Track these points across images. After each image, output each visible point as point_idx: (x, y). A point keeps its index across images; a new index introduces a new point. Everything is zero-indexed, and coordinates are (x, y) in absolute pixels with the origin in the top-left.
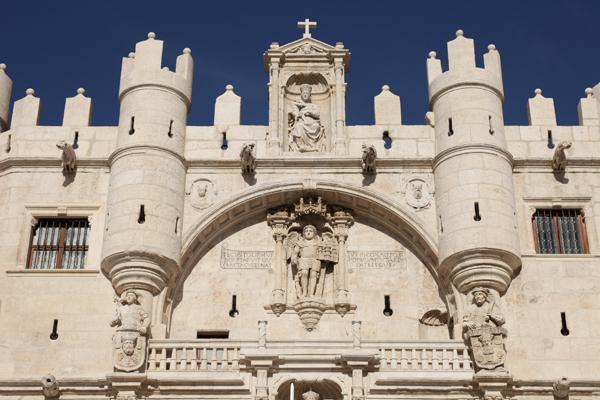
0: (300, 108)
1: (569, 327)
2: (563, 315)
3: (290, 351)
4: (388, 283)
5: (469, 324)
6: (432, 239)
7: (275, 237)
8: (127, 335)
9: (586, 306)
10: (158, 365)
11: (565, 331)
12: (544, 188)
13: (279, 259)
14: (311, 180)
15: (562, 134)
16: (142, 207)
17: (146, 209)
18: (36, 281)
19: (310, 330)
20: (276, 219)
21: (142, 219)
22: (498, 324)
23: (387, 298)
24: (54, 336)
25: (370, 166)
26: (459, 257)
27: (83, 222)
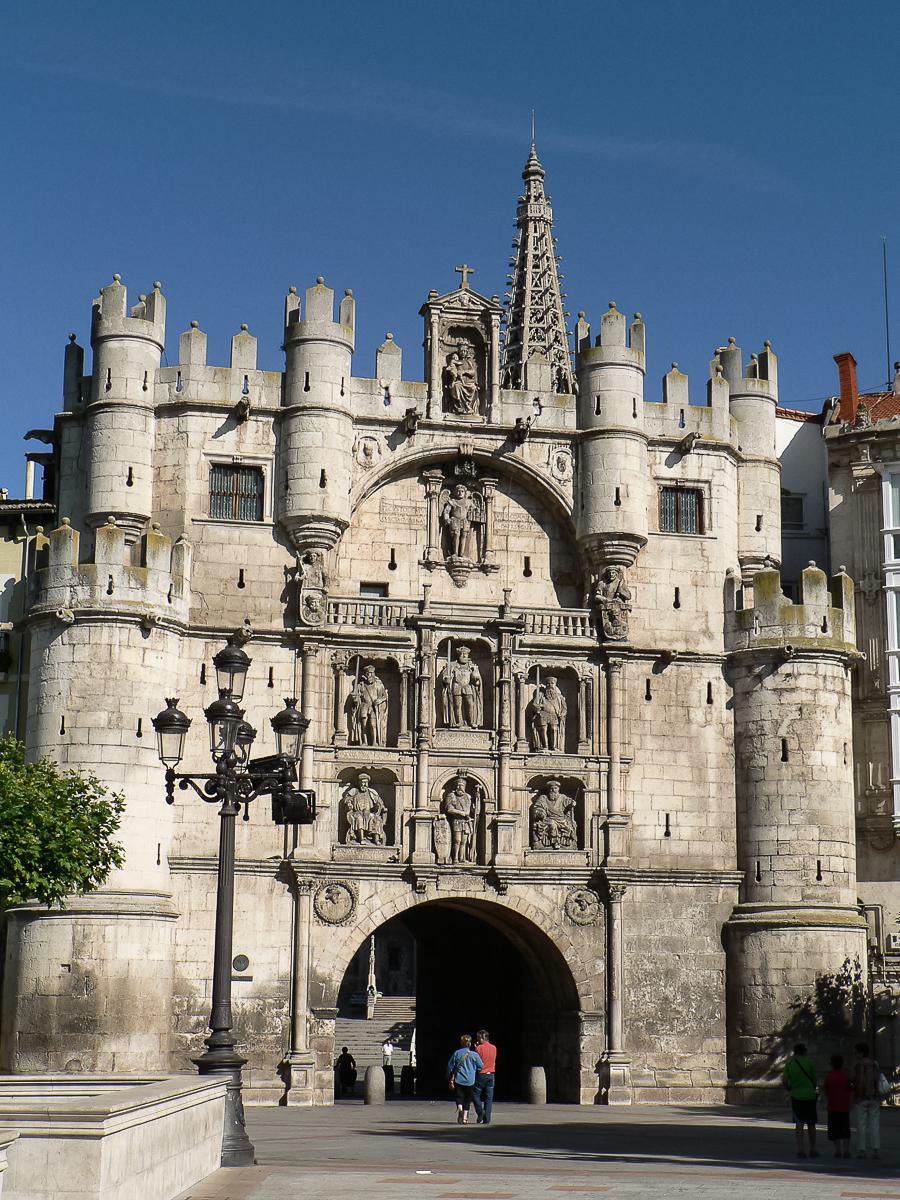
1: (681, 600)
2: (677, 590)
3: (449, 612)
6: (570, 509)
8: (312, 593)
10: (336, 619)
11: (677, 605)
16: (323, 471)
17: (327, 473)
18: (221, 532)
19: (459, 587)
20: (432, 477)
21: (323, 484)
22: (624, 598)
23: (527, 560)
24: (241, 585)
25: (517, 435)
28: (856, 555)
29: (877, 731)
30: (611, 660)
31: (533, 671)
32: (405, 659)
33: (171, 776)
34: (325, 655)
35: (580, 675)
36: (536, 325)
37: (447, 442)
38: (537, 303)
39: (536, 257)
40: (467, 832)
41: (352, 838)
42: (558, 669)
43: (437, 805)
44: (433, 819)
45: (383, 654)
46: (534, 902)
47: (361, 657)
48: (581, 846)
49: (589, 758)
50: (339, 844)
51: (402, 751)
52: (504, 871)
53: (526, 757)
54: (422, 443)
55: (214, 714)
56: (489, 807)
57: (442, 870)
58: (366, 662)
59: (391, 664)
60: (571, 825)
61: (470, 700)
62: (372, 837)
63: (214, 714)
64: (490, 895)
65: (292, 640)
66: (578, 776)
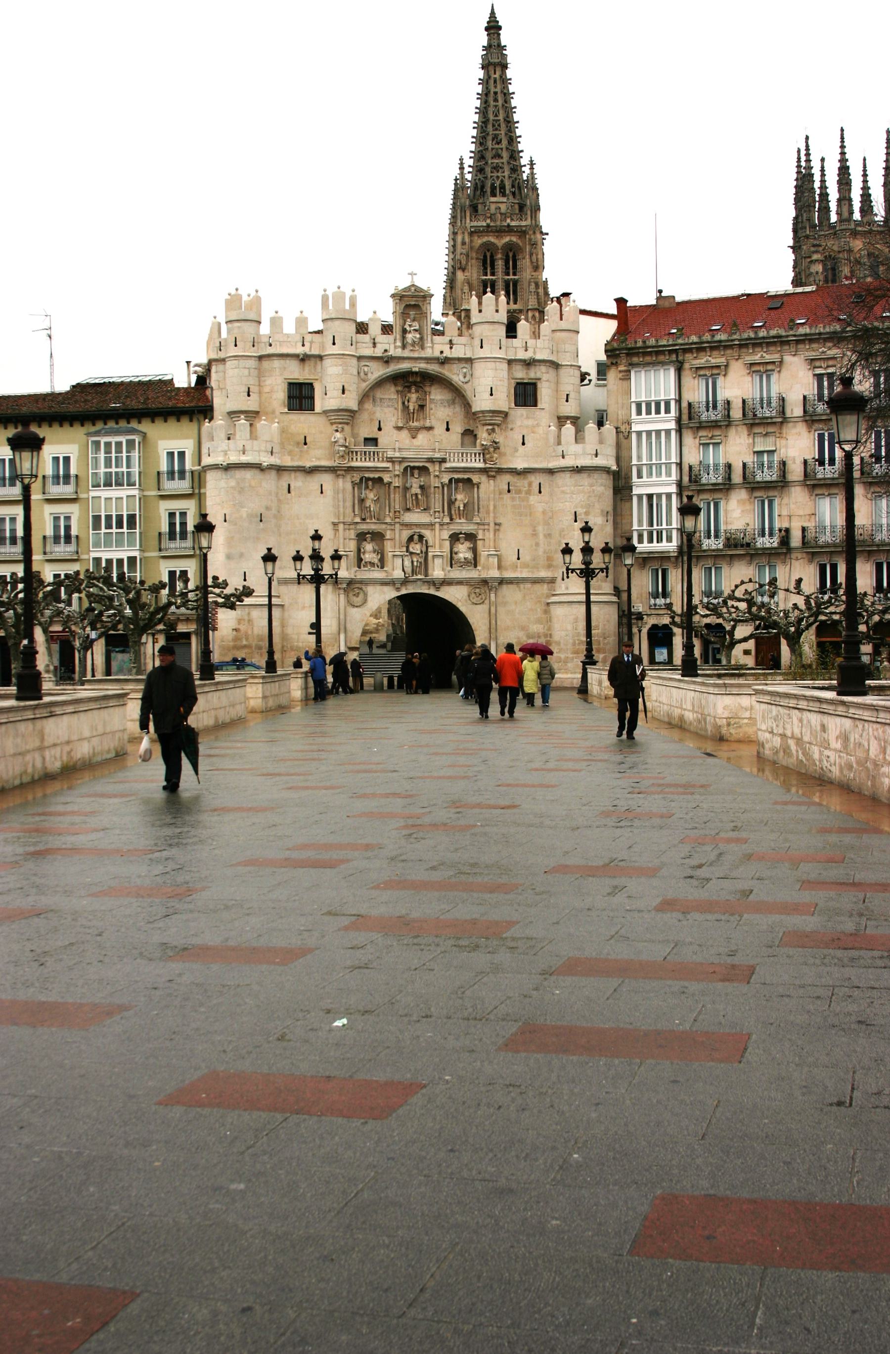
0: (410, 326)
1: (526, 442)
4: (448, 415)
5: (485, 443)
7: (397, 391)
9: (533, 432)
11: (523, 444)
12: (521, 374)
13: (400, 403)
14: (417, 367)
15: (531, 342)
19: (414, 437)
21: (343, 392)
22: (496, 443)
24: (305, 444)
26: (483, 412)
27: (311, 385)
28: (620, 413)
29: (627, 504)
31: (450, 480)
32: (386, 478)
33: (299, 575)
34: (348, 478)
35: (474, 482)
36: (497, 146)
37: (405, 366)
38: (496, 129)
39: (496, 93)
43: (405, 549)
45: (376, 476)
46: (455, 595)
48: (475, 566)
54: (393, 368)
55: (311, 557)
58: (368, 479)
59: (380, 480)
60: (469, 555)
61: (420, 497)
62: (372, 564)
63: (311, 557)
64: (432, 591)
65: (331, 470)
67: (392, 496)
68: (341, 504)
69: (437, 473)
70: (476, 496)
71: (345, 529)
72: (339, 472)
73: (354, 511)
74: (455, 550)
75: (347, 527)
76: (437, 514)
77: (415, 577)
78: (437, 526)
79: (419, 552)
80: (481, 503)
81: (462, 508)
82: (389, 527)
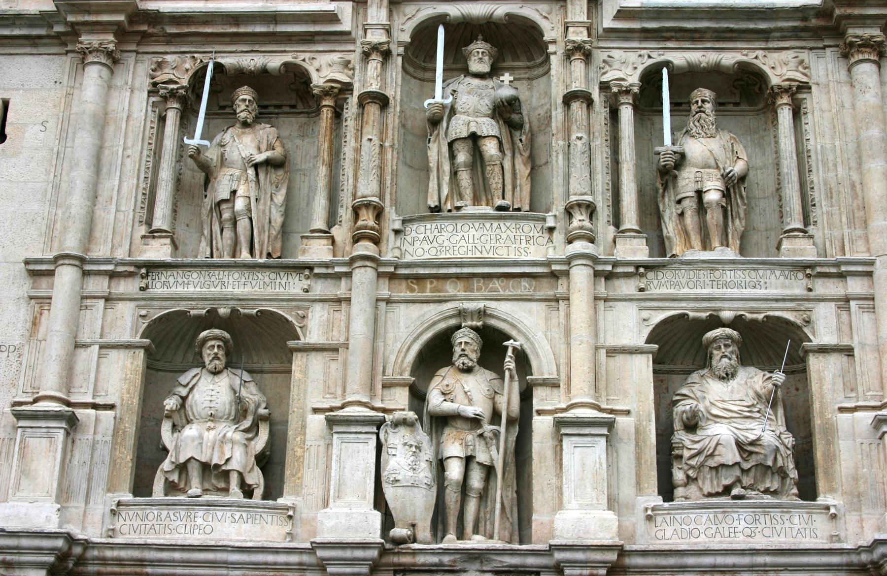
30: (854, 32)
31: (651, 77)
35: (775, 81)
40: (482, 457)
41: (171, 488)
42: (716, 70)
43: (400, 399)
44: (379, 424)
45: (275, 62)
47: (218, 67)
49: (811, 266)
50: (129, 497)
51: (310, 267)
52: (579, 556)
53: (642, 269)
56: (541, 399)
57: (406, 560)
61: (490, 148)
66: (789, 316)
67: (348, 150)
68: (81, 175)
69: (579, 35)
70: (787, 142)
71: (84, 300)
72: (88, 39)
73: (149, 223)
74: (683, 407)
75: (98, 285)
76: (580, 219)
77: (451, 541)
78: (581, 275)
79: (478, 408)
80: (817, 178)
81: (713, 197)
82: (320, 288)
